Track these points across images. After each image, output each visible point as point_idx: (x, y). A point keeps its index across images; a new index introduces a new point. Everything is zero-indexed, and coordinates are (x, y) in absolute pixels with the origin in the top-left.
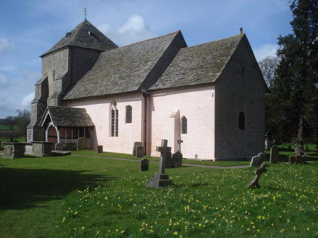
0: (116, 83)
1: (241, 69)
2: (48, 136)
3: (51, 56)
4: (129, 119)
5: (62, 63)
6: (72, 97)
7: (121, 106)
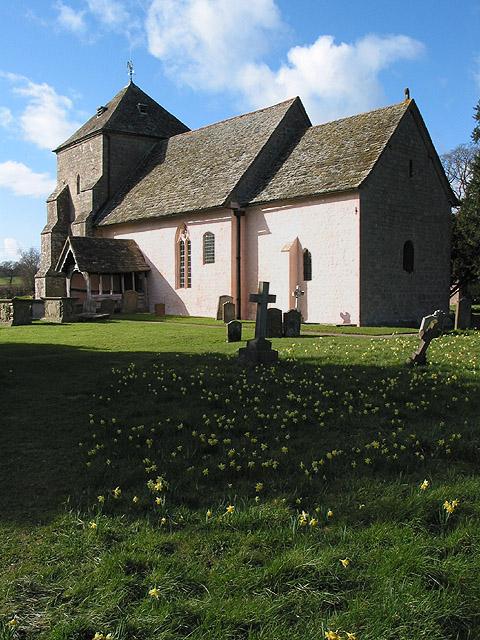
0: (187, 193)
1: (408, 164)
2: (71, 290)
3: (73, 150)
5: (92, 163)
7: (196, 232)
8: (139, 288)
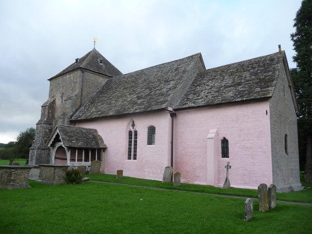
0: (136, 103)
2: (56, 158)
3: (60, 79)
4: (151, 141)
6: (83, 118)
7: (142, 126)
8: (99, 159)
